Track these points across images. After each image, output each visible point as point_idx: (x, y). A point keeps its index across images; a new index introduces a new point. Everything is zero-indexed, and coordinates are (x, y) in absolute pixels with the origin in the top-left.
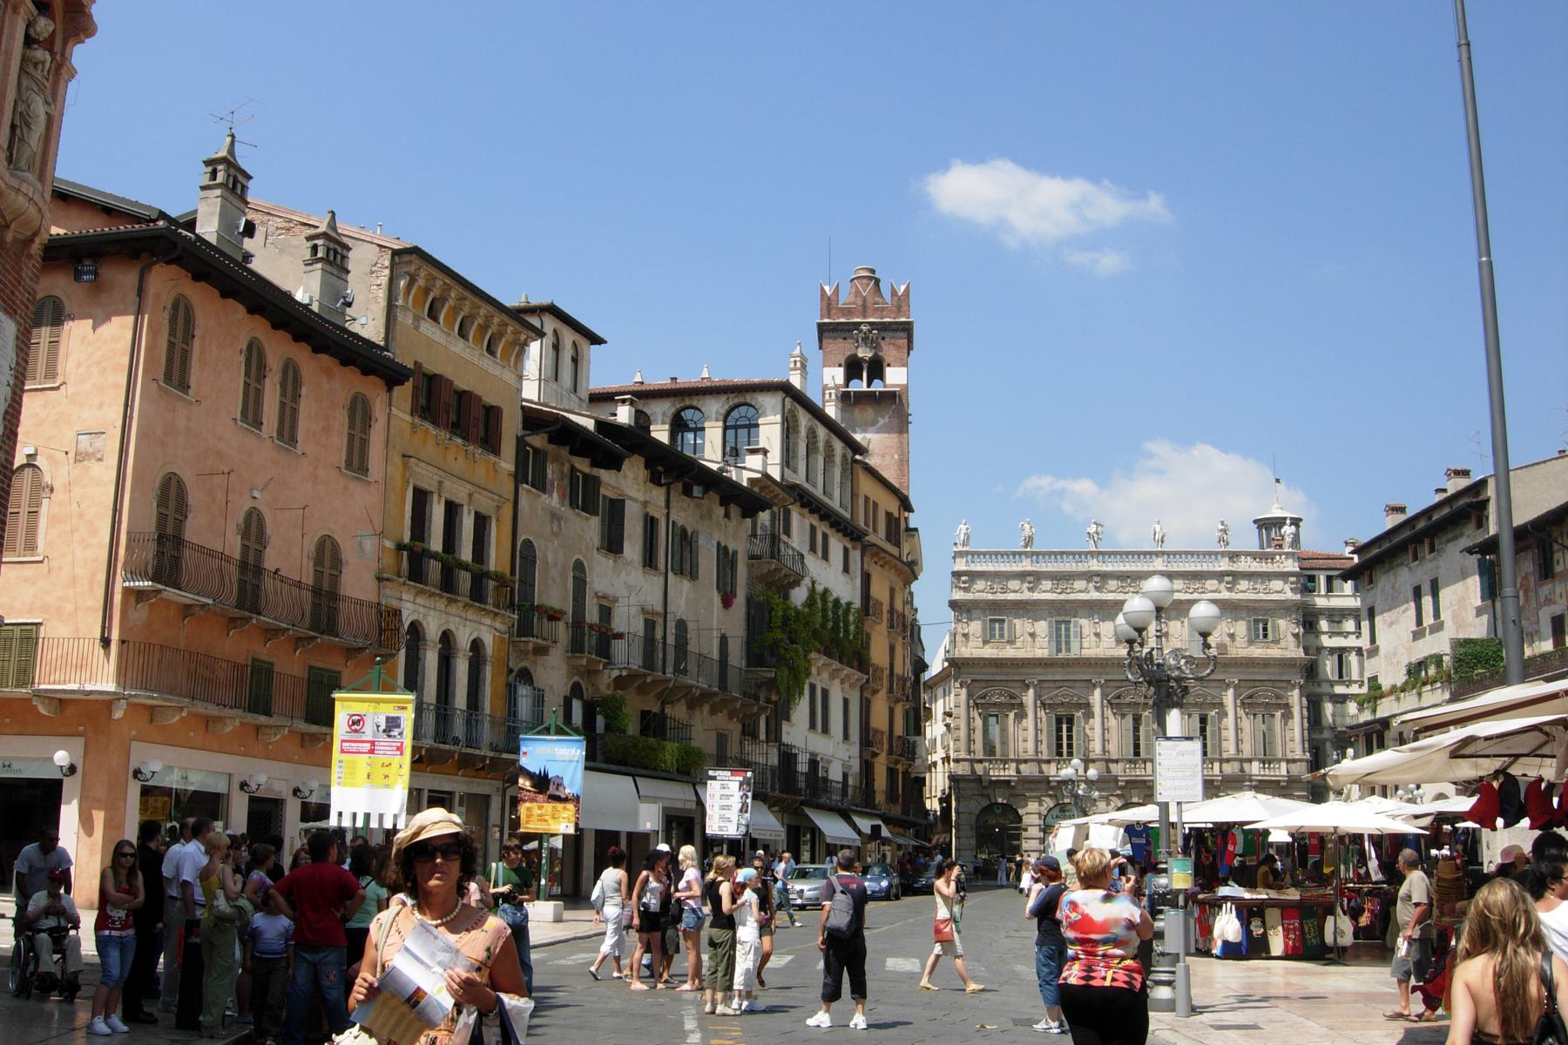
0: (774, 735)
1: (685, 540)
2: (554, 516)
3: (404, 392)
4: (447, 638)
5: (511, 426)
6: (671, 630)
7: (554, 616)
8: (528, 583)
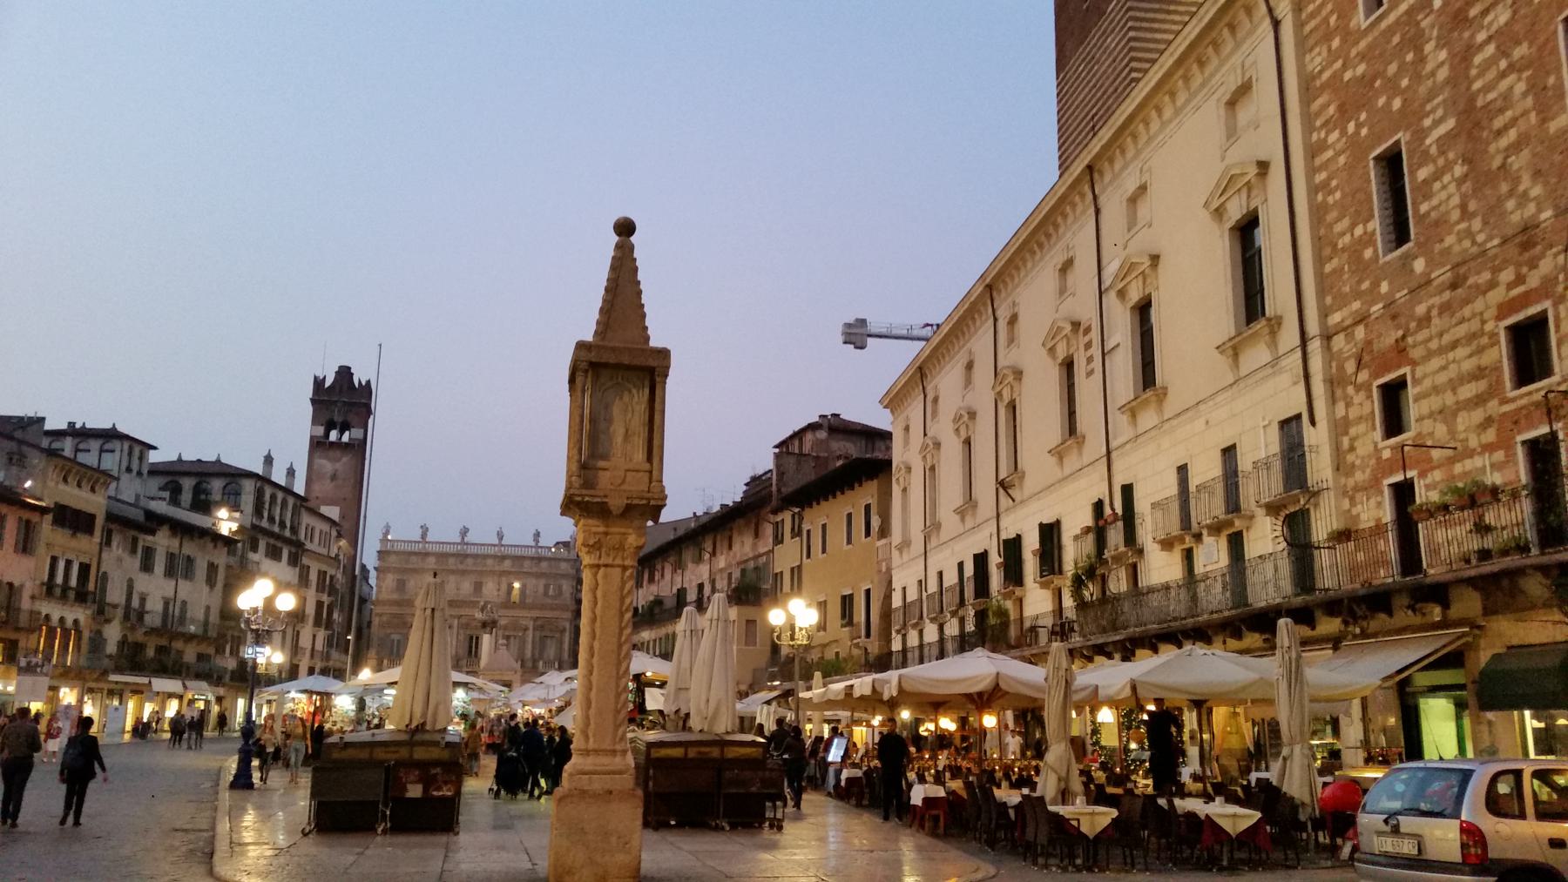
0: (235, 652)
1: (190, 560)
2: (120, 560)
3: (49, 517)
4: (62, 620)
5: (100, 522)
6: (178, 604)
7: (115, 606)
8: (104, 590)
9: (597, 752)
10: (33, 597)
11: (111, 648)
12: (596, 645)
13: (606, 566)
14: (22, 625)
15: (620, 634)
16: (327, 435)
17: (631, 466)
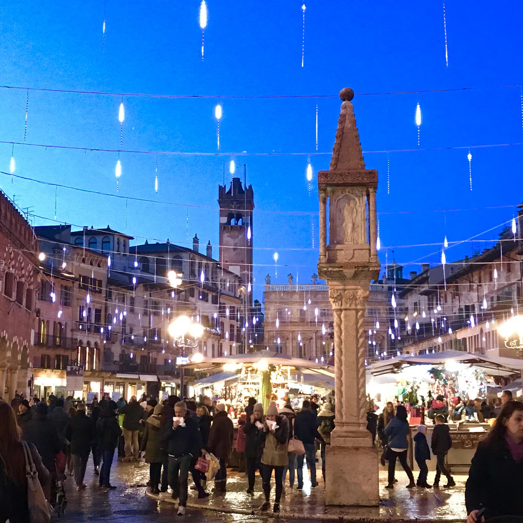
4: (88, 343)
9: (348, 424)
10: (72, 330)
11: (116, 358)
12: (343, 358)
13: (346, 309)
14: (67, 347)
15: (358, 352)
16: (229, 222)
17: (356, 247)
